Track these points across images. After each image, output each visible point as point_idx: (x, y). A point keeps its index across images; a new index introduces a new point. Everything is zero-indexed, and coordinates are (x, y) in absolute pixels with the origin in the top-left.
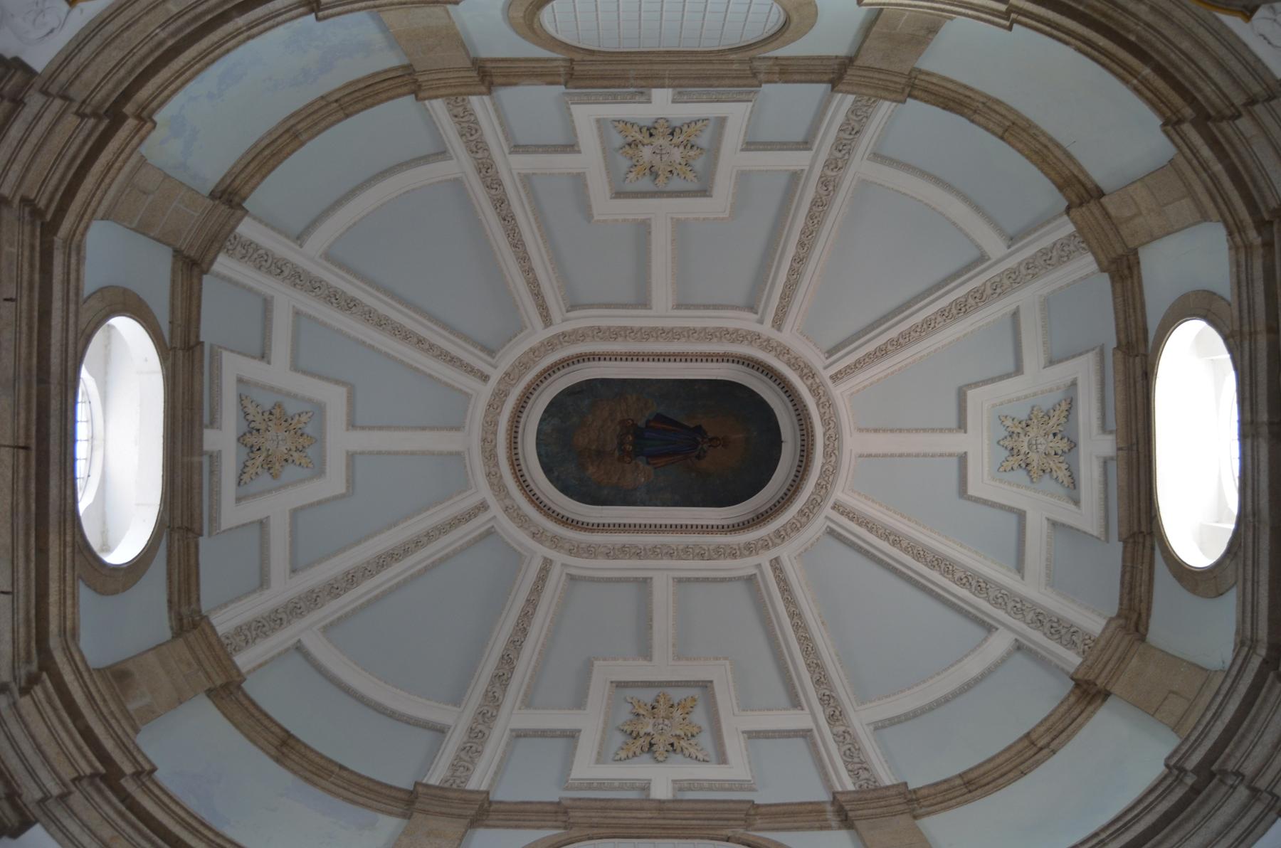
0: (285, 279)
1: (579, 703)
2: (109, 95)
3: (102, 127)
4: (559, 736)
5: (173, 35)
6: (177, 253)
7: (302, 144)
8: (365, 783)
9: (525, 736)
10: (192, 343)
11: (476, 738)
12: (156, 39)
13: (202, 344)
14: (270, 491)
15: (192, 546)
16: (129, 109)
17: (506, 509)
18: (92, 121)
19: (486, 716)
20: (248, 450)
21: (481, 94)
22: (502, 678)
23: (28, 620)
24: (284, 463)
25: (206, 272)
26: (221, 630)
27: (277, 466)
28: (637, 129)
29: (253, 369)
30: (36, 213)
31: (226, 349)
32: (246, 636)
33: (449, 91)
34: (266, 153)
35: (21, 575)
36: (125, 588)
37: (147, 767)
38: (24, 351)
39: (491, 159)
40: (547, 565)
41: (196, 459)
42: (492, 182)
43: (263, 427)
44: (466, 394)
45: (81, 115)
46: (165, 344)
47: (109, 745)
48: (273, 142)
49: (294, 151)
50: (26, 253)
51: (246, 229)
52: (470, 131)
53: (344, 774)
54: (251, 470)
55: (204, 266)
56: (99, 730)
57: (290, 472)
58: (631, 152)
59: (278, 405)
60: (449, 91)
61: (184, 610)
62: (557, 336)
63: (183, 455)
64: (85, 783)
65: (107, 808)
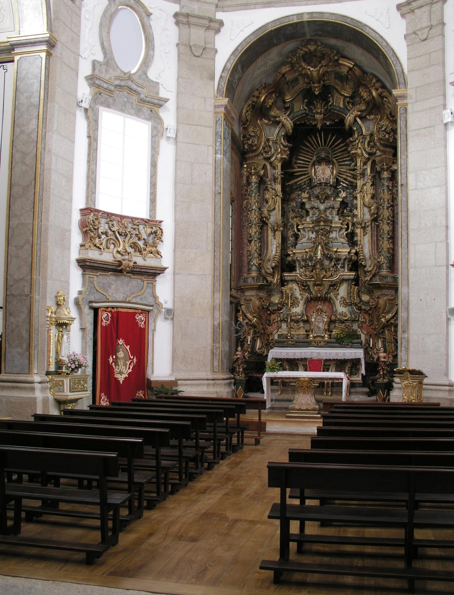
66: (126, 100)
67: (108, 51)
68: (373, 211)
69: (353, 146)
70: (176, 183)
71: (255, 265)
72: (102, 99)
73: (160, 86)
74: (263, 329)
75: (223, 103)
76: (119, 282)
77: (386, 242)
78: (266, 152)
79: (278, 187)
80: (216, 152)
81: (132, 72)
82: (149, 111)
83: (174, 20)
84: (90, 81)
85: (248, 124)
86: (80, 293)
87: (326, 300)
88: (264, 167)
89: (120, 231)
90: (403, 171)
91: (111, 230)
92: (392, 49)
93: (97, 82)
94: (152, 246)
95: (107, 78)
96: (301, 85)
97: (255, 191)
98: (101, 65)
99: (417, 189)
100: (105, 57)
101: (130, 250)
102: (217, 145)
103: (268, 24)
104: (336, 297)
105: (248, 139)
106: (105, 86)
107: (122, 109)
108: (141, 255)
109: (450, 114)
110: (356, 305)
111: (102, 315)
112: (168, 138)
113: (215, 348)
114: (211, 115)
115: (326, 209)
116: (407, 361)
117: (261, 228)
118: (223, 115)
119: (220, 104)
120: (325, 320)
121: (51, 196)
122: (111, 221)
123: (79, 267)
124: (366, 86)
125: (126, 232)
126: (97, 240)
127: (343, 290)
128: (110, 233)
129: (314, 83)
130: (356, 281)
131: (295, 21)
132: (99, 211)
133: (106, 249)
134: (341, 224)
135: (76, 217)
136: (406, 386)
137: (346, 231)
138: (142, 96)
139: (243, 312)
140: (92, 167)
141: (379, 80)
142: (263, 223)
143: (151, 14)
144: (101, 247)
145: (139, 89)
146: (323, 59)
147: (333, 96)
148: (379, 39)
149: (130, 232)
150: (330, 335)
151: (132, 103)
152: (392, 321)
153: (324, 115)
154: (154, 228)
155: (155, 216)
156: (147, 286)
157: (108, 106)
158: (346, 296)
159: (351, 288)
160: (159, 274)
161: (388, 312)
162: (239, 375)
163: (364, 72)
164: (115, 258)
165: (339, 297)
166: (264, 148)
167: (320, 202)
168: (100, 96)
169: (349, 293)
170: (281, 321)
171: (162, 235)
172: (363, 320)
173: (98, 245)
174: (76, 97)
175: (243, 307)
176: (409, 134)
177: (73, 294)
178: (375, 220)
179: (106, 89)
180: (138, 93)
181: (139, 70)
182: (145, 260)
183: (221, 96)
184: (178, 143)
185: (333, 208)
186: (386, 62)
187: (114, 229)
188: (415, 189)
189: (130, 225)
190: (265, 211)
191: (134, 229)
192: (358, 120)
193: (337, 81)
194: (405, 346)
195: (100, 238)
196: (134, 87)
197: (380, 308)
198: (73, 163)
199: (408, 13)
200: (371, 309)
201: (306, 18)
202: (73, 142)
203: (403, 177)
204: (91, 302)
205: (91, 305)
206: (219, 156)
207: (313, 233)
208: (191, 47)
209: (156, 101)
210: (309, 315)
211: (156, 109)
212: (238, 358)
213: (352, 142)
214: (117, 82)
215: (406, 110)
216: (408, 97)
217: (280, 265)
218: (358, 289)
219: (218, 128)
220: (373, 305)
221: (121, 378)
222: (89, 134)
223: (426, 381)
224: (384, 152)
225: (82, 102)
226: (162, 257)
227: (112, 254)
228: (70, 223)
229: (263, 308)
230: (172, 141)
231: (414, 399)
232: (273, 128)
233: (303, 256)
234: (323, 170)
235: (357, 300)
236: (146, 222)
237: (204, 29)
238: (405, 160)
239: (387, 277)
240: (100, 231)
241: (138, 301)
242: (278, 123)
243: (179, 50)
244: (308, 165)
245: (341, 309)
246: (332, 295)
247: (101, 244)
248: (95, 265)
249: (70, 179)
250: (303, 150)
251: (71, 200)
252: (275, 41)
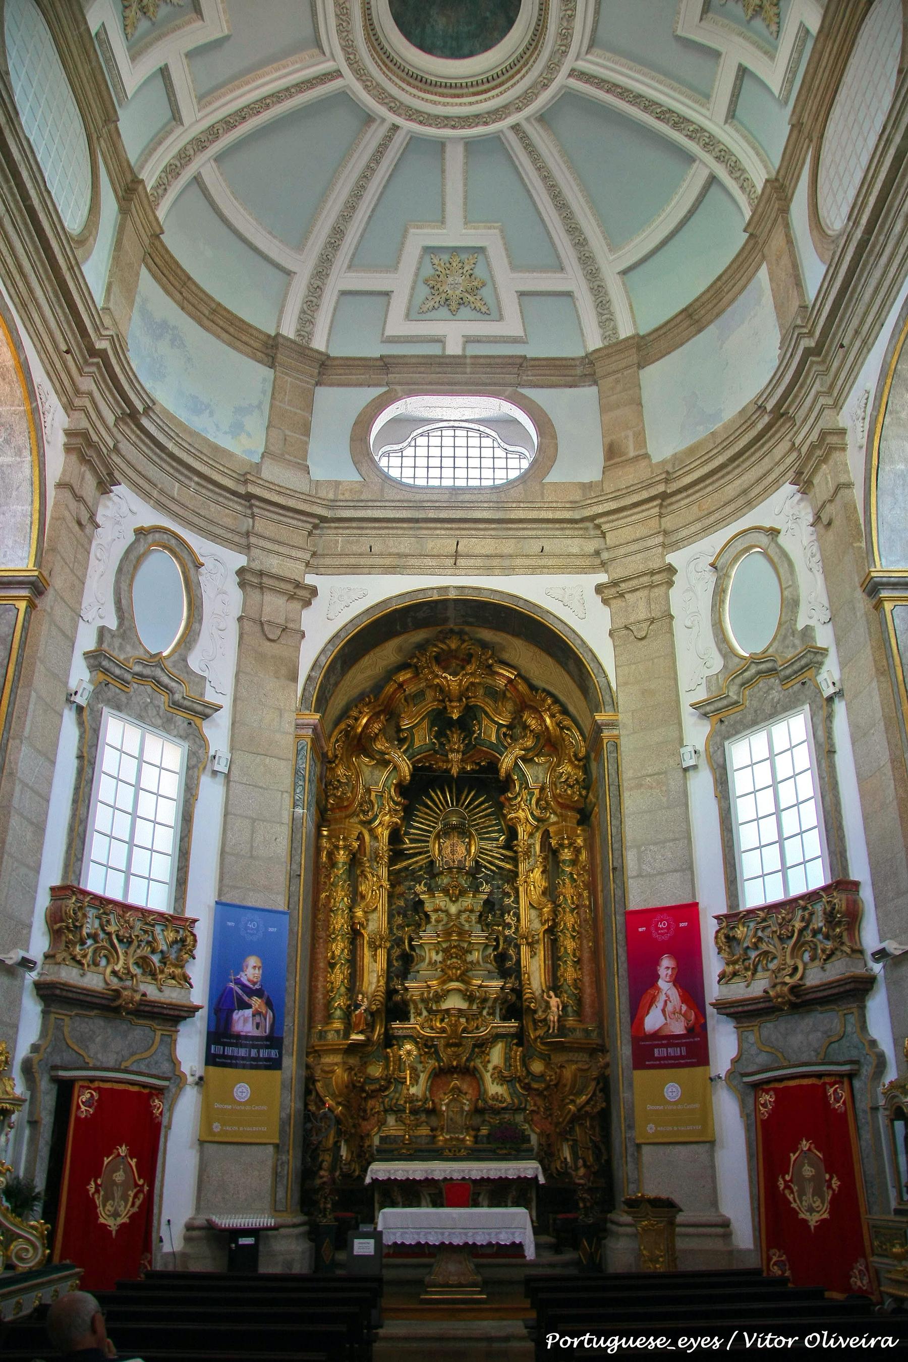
0: (323, 283)
1: (716, 55)
2: (237, 502)
3: (257, 503)
4: (742, 81)
5: (190, 479)
6: (318, 384)
7: (219, 304)
8: (735, 266)
9: (734, 111)
10: (381, 363)
11: (724, 156)
12: (197, 488)
13: (382, 358)
14: (495, 289)
15: (533, 363)
16: (242, 490)
17: (519, 109)
18: (256, 510)
19: (710, 143)
20: (462, 307)
21: (145, 188)
22: (680, 122)
23: (562, 529)
24: (473, 277)
25: (328, 357)
26: (599, 345)
27: (475, 283)
28: (128, 11)
29: (399, 305)
30: (316, 527)
31: (383, 334)
32: (607, 320)
33: (150, 213)
34: (231, 330)
35: (534, 533)
36: (554, 437)
37: (664, 476)
38: (400, 532)
39: (192, 141)
40: (574, 73)
41: (468, 361)
42: (213, 134)
43: (444, 296)
44: (411, 138)
45: (253, 516)
46: (385, 393)
47: (645, 495)
48: (222, 328)
49: (225, 309)
50: (341, 531)
51: (289, 330)
52: (172, 171)
53: (724, 278)
54: (478, 305)
55: (324, 358)
56: (635, 498)
57: (480, 272)
58: (152, 9)
59: (426, 282)
60: (150, 213)
61: (579, 371)
62: (350, 65)
63: (465, 373)
64: (663, 511)
65: (683, 503)
66: (149, 700)
67: (126, 615)
68: (546, 916)
69: (512, 806)
70: (223, 853)
71: (341, 1008)
72: (110, 694)
73: (207, 682)
74: (354, 1126)
75: (312, 721)
76: (109, 1030)
77: (570, 969)
78: (365, 813)
79: (384, 872)
81: (165, 654)
82: (186, 724)
83: (238, 580)
84: (92, 661)
85: (337, 762)
86: (35, 1048)
87: (470, 1073)
88: (360, 838)
89: (121, 933)
90: (616, 846)
91: (104, 930)
92: (591, 650)
93: (105, 663)
94: (176, 966)
95: (122, 657)
96: (430, 704)
97: (344, 877)
98: (113, 636)
99: (642, 876)
100: (120, 625)
101: (135, 970)
102: (298, 791)
103: (391, 598)
104: (485, 1067)
105: (337, 788)
106: (117, 671)
107: (141, 717)
108: (153, 982)
109: (693, 752)
110: (520, 1081)
111: (79, 1096)
112: (215, 773)
113: (279, 1162)
114: (291, 739)
115: (460, 912)
116: (639, 1182)
117: (353, 942)
118: (309, 740)
119: (306, 721)
120: (466, 1108)
121: (6, 856)
122: (105, 913)
123: (37, 999)
124: (536, 711)
125: (131, 937)
126: (78, 948)
127: (497, 1055)
128: (102, 935)
129: (450, 701)
130: (520, 1037)
131: (436, 597)
132: (85, 893)
133: (93, 968)
134: (487, 938)
135: (43, 901)
136: (645, 1230)
137: (494, 950)
138: (177, 697)
139: (318, 1094)
140: (83, 810)
141: (556, 701)
142: (355, 935)
143: (203, 565)
144: (84, 961)
145: (173, 684)
146: (469, 662)
147: (480, 723)
148: (569, 634)
149: (137, 936)
150: (476, 1137)
151: (159, 707)
152: (588, 1108)
153: (463, 754)
154: (181, 931)
155: (183, 911)
156: (161, 1040)
157: (118, 708)
158: (502, 1065)
159: (511, 1050)
160: (185, 1018)
161: (580, 1093)
162: (325, 1216)
163: (532, 687)
164: (107, 984)
165: (490, 1067)
166: (361, 805)
167: (451, 900)
168: (106, 689)
169: (507, 1059)
170: (386, 1111)
171: (194, 946)
172: (533, 1108)
173: (79, 958)
174: (66, 684)
175: (319, 1085)
176: (625, 785)
177: (22, 1051)
178: (550, 931)
179: (117, 677)
180: (171, 691)
181: (174, 651)
182: (160, 990)
183: (307, 709)
184: (232, 783)
185: (472, 911)
186: (580, 670)
187: (111, 929)
188: (638, 876)
189: (138, 925)
190: (359, 913)
191: (146, 932)
192: (520, 762)
194: (633, 1154)
195: (83, 943)
196: (165, 680)
197: (565, 1086)
198: (48, 801)
199: (615, 598)
200: (548, 1087)
201: (452, 595)
202: (53, 763)
203: (616, 856)
204: (55, 1068)
205: (53, 1073)
206: (299, 811)
207: (437, 953)
208: (262, 624)
209: (199, 708)
210: (437, 1100)
211: (198, 721)
212: (324, 1183)
213: (510, 799)
214: (137, 669)
215: (616, 746)
216: (621, 726)
217: (384, 1008)
218: (522, 1051)
219: (300, 762)
220: (551, 1080)
221: (113, 1224)
222: (82, 752)
223: (680, 1218)
224: (563, 817)
225: (76, 693)
226: (191, 986)
227: (101, 976)
228: (32, 912)
229: (354, 1086)
230: (220, 779)
231: (661, 1256)
232: (376, 772)
233: (423, 994)
235: (520, 1071)
236: (167, 920)
237: (286, 598)
238: (617, 828)
239: (575, 1029)
240: (85, 931)
241: (143, 1068)
242: (386, 763)
243: (241, 628)
245: (494, 1089)
246: (478, 1063)
247: (85, 956)
248: (70, 995)
249: (40, 829)
250: (419, 811)
251: (37, 870)
252: (398, 627)
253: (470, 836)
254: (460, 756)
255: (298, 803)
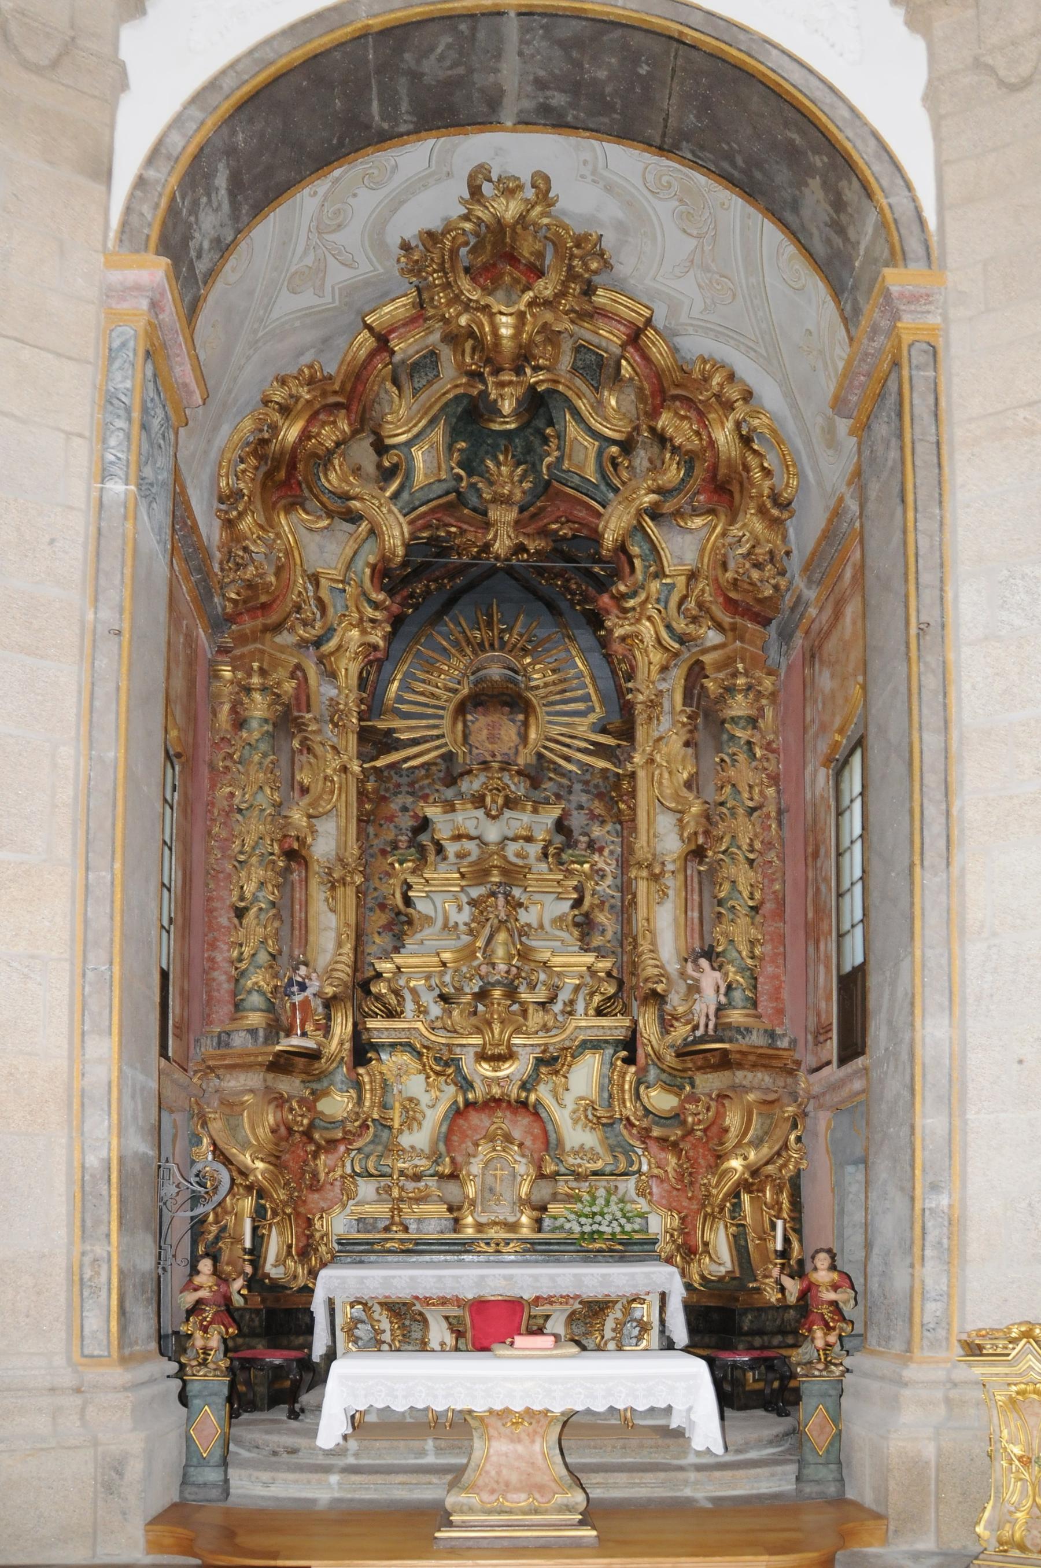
80: (104, 470)
102: (113, 442)
137: (573, 907)
153: (522, 510)
167: (488, 815)
193: (578, 382)
207: (460, 909)
234: (492, 726)
244: (441, 717)
253: (527, 708)
254: (512, 515)
255: (114, 469)
